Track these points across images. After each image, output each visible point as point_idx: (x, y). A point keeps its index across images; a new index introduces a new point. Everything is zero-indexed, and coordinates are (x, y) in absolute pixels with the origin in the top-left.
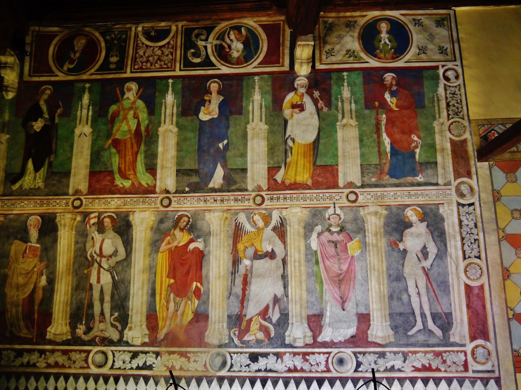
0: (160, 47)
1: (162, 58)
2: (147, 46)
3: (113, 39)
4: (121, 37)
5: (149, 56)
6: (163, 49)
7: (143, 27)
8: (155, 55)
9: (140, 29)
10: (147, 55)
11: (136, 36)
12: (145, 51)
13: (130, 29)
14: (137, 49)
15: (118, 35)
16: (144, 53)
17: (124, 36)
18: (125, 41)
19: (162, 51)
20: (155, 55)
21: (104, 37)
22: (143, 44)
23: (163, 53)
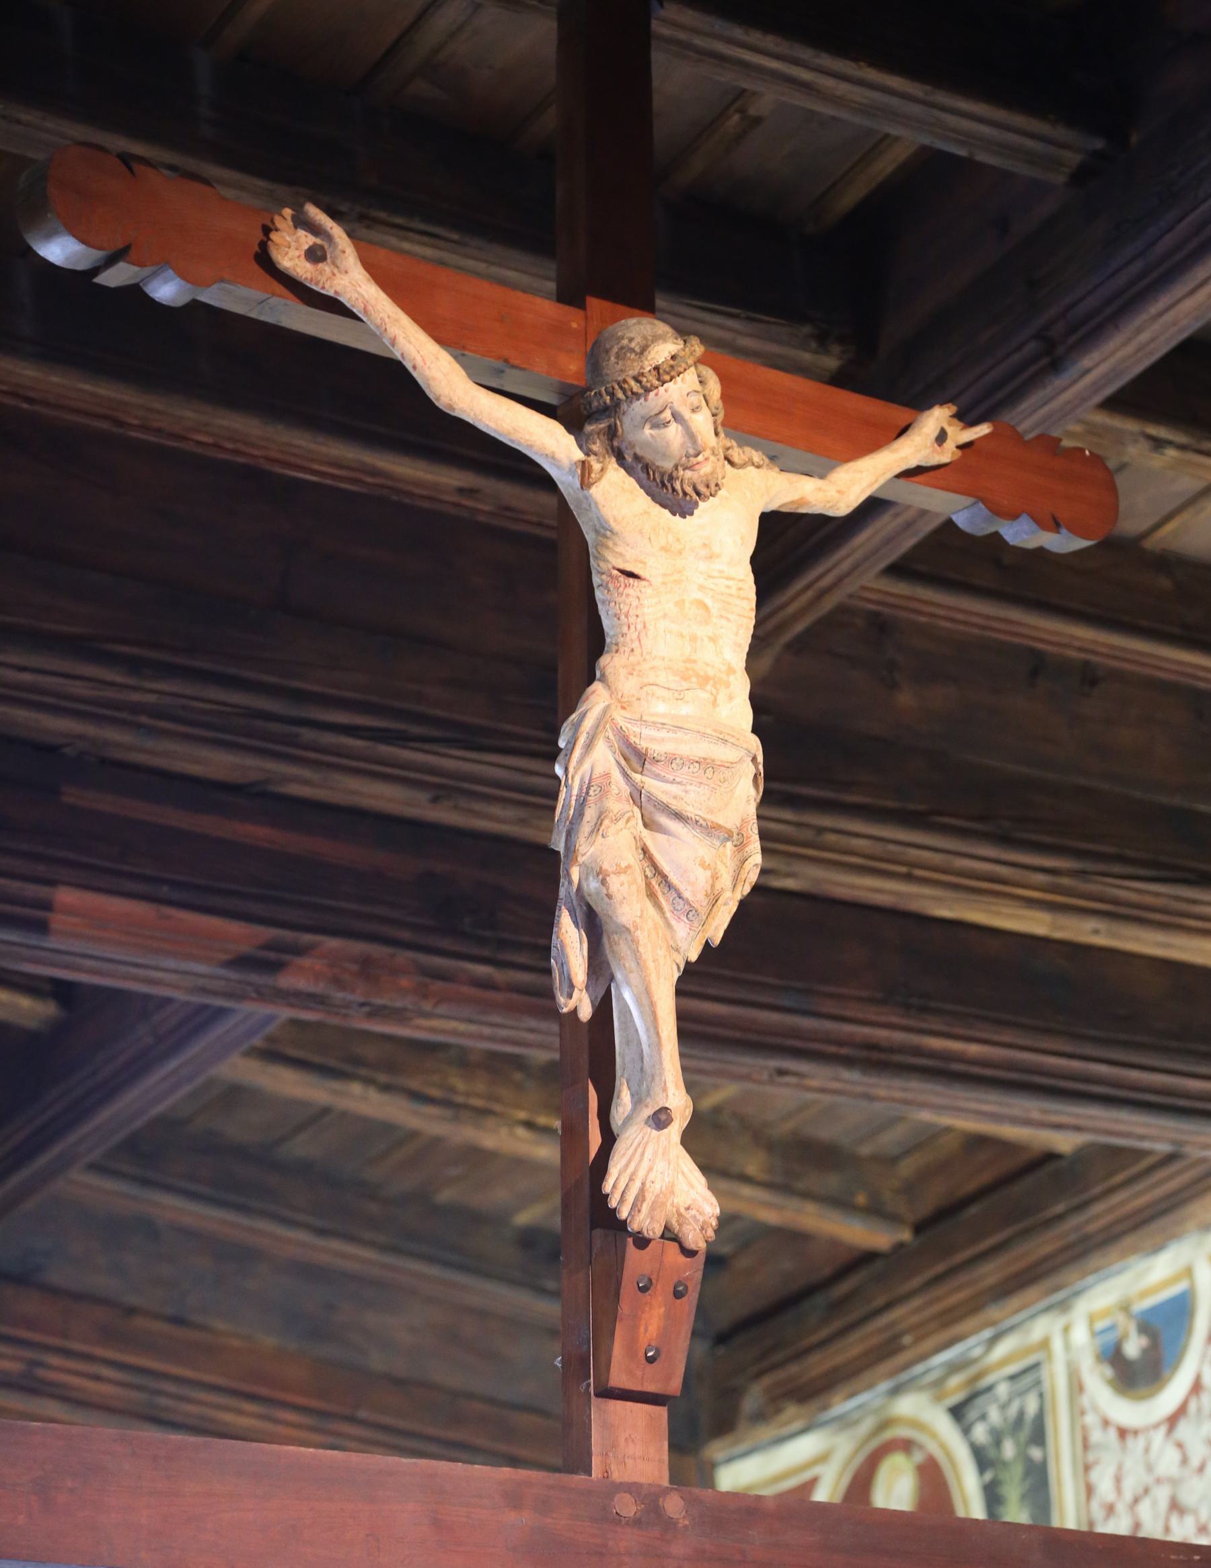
0: (1173, 1420)
1: (1188, 1497)
2: (1123, 1433)
3: (997, 1437)
4: (1021, 1414)
5: (1136, 1501)
6: (1184, 1430)
7: (1092, 1319)
8: (1159, 1481)
9: (1080, 1335)
10: (1128, 1496)
11: (1077, 1387)
12: (1120, 1467)
13: (1045, 1344)
14: (1087, 1468)
15: (1010, 1401)
16: (1118, 1480)
17: (1032, 1406)
18: (1039, 1436)
19: (1180, 1446)
20: (1159, 1481)
21: (966, 1431)
22: (1106, 1423)
23: (1185, 1461)
